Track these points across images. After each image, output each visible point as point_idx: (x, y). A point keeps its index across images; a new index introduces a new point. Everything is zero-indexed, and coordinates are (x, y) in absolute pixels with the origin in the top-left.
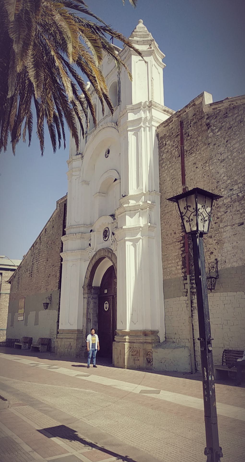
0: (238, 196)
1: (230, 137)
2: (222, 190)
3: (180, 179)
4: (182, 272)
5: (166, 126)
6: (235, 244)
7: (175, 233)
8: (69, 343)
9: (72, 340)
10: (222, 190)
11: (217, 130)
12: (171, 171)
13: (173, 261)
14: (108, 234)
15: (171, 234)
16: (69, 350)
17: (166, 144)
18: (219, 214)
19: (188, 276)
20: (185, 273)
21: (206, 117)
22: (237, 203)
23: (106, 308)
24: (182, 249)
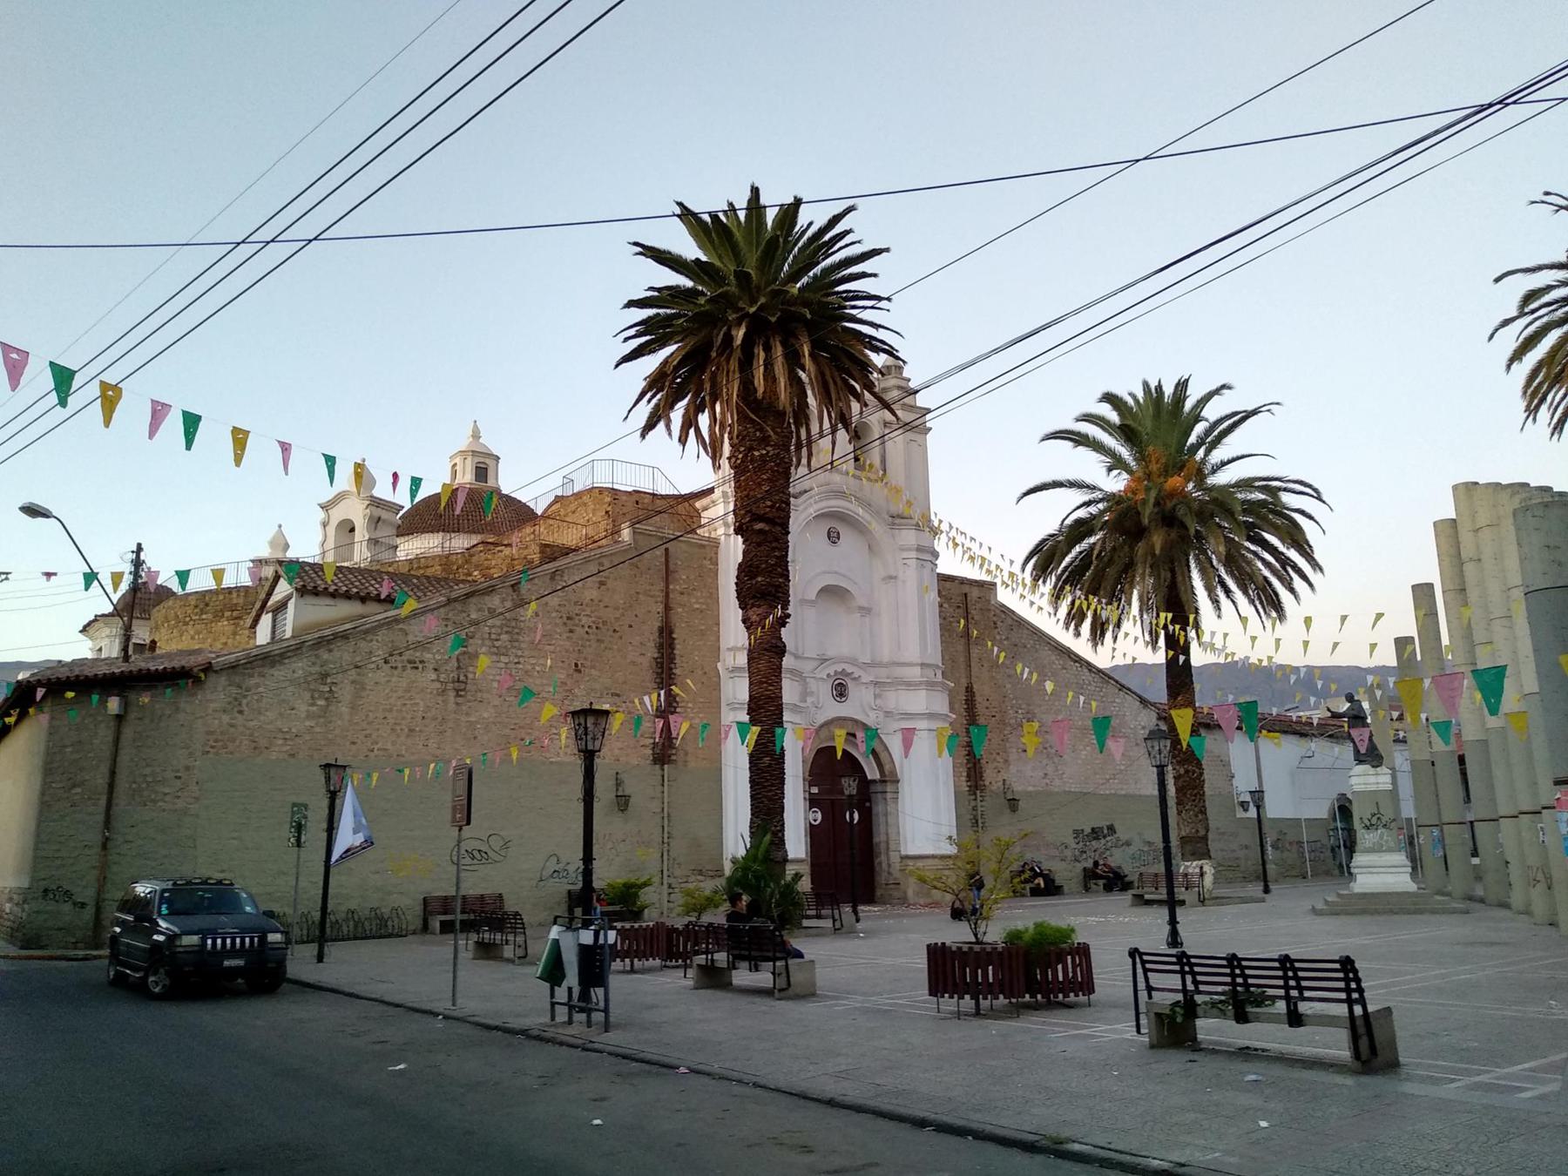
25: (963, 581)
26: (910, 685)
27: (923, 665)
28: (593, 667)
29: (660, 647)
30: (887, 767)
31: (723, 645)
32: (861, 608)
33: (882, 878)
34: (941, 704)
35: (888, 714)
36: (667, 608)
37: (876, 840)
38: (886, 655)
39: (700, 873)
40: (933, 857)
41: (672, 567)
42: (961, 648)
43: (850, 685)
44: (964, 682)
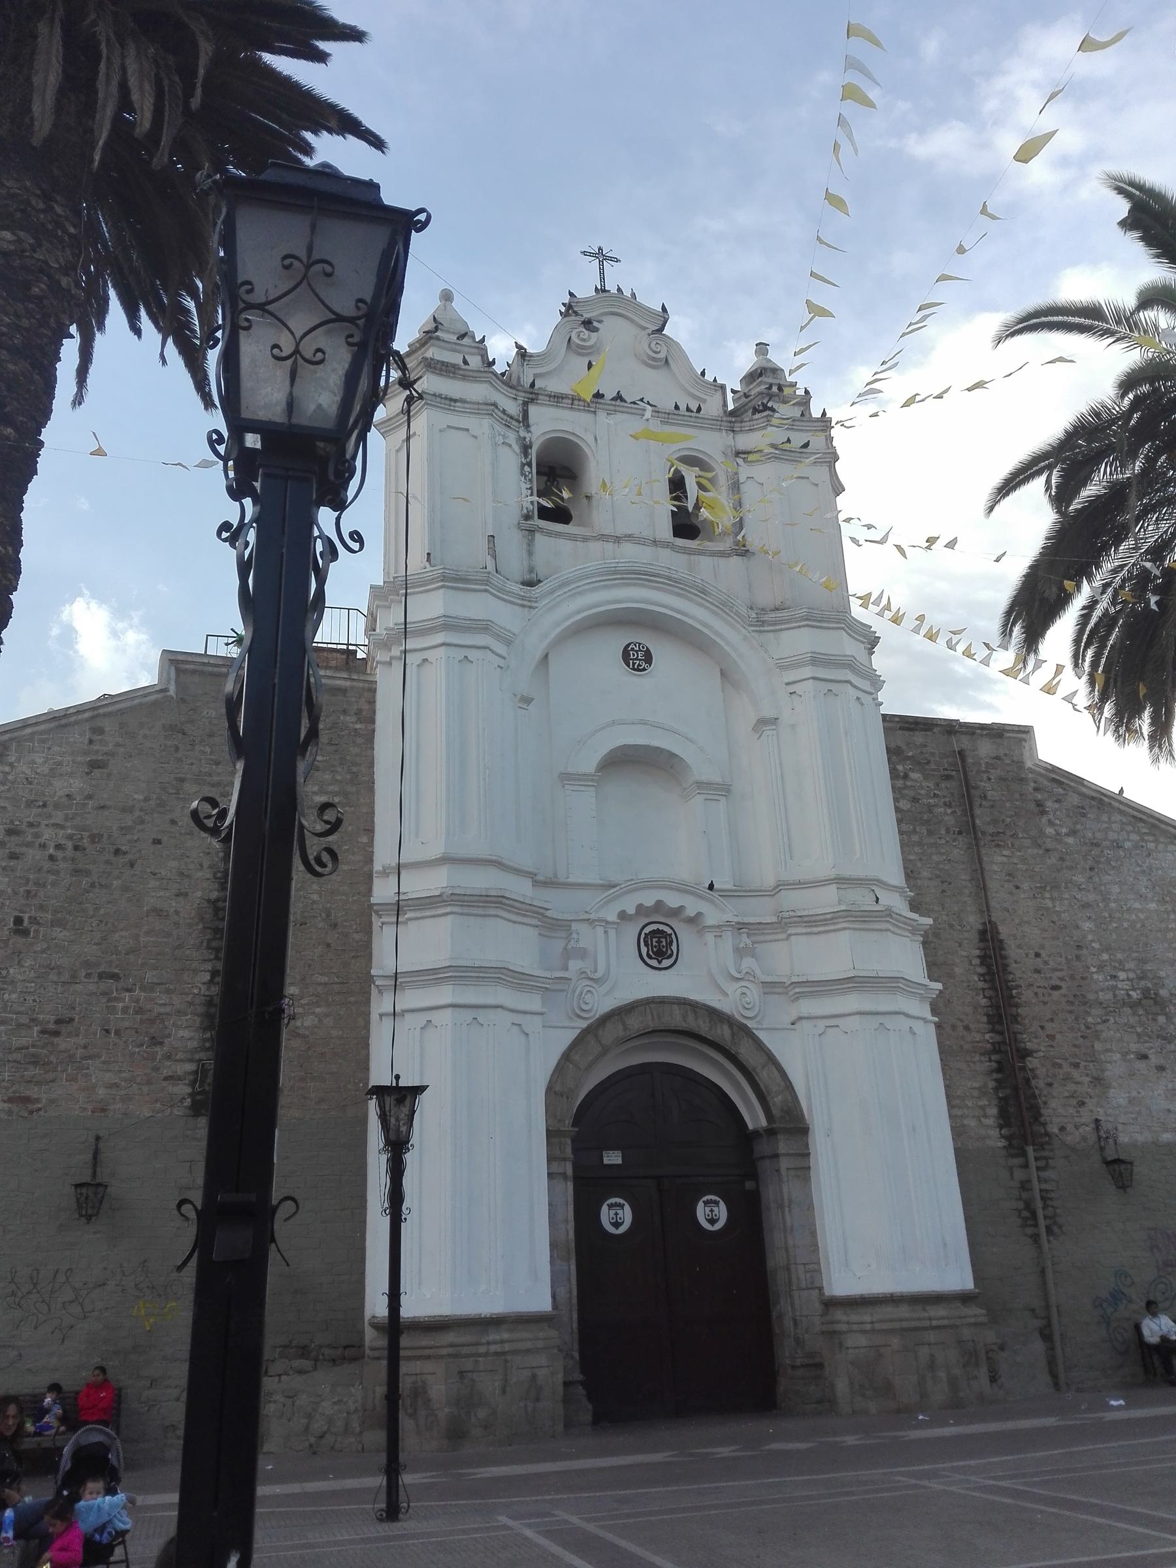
0: (1128, 995)
1: (1098, 862)
3: (967, 891)
4: (1002, 1136)
6: (1134, 1094)
7: (967, 1028)
9: (542, 1360)
10: (1094, 970)
11: (1064, 830)
12: (935, 858)
14: (674, 948)
15: (954, 1027)
17: (906, 777)
19: (1030, 1149)
23: (617, 1225)
24: (995, 1076)
26: (813, 923)
27: (841, 881)
28: (57, 923)
30: (778, 1099)
33: (786, 1353)
34: (905, 958)
35: (770, 987)
37: (770, 1264)
38: (765, 873)
39: (304, 1352)
43: (686, 937)
44: (973, 921)
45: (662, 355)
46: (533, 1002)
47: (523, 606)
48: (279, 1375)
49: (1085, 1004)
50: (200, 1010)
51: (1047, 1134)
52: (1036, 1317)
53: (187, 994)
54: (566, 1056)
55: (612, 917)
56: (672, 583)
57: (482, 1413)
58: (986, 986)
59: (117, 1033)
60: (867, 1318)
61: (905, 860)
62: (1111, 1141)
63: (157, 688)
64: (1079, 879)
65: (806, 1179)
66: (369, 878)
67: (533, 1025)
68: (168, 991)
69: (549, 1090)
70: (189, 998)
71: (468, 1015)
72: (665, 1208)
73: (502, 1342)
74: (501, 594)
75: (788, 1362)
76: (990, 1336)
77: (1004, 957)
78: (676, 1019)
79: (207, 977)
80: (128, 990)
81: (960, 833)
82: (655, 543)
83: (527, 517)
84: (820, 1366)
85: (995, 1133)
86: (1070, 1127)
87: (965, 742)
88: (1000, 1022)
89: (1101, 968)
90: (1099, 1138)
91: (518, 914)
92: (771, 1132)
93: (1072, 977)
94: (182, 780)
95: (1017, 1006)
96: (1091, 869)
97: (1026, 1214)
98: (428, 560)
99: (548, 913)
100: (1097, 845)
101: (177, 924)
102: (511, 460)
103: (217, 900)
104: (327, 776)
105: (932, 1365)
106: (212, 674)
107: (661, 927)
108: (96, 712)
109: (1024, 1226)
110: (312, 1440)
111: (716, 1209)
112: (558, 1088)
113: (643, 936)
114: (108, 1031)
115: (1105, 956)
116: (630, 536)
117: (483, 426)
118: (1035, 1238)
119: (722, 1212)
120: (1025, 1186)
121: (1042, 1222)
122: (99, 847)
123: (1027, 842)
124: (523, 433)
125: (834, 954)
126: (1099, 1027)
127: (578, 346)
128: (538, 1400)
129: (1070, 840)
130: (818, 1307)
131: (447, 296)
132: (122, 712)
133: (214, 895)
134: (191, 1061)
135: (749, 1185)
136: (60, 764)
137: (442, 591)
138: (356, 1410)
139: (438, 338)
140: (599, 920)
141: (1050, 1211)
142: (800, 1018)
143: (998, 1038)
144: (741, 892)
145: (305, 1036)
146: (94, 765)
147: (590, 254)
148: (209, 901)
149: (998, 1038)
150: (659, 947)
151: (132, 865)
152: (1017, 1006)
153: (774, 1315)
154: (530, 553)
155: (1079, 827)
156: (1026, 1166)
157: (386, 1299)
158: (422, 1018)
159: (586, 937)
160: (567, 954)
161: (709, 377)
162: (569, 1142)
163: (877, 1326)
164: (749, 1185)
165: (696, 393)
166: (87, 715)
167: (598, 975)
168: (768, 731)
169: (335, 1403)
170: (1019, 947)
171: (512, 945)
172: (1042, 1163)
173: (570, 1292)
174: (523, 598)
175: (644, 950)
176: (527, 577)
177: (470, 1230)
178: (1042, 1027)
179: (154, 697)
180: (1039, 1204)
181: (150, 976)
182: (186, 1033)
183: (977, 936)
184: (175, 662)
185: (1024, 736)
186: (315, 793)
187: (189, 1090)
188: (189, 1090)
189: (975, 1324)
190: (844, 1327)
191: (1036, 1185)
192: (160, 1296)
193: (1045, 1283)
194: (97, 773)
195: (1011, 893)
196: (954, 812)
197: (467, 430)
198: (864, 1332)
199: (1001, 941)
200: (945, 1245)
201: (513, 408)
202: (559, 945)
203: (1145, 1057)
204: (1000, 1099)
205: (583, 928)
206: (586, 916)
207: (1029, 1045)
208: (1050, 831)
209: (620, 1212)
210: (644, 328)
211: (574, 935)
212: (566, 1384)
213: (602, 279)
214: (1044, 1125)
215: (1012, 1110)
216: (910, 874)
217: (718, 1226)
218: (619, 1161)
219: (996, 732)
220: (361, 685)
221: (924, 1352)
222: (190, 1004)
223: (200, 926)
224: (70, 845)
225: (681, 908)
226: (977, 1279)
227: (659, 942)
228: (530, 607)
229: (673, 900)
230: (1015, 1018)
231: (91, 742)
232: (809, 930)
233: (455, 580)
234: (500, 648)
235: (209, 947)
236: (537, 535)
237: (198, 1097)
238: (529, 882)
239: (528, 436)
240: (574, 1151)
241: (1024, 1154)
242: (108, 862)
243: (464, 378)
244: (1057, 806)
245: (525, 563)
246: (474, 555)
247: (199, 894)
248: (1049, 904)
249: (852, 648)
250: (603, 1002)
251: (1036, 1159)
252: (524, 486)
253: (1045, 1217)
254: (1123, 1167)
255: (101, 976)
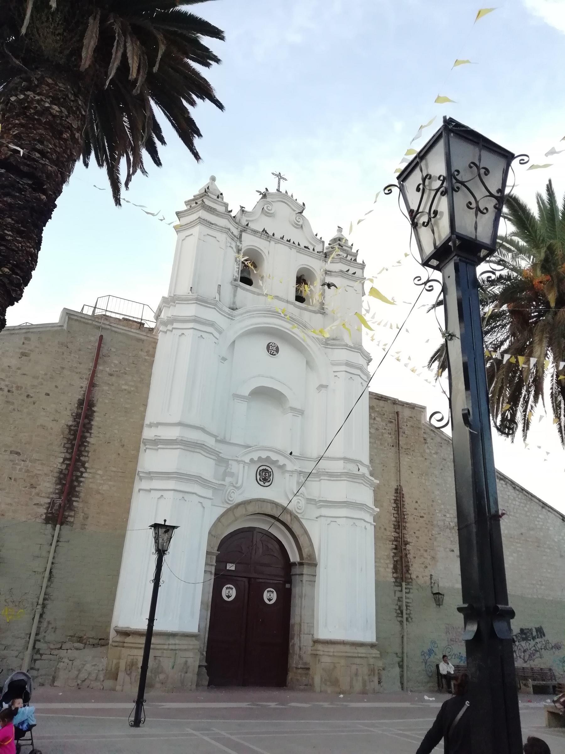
2: (437, 511)
5: (378, 399)
7: (385, 529)
8: (184, 660)
9: (191, 654)
10: (437, 511)
11: (433, 452)
13: (382, 561)
14: (271, 478)
16: (183, 675)
17: (374, 419)
18: (433, 532)
19: (404, 584)
20: (396, 578)
21: (423, 431)
22: (448, 530)
23: (228, 597)
25: (395, 402)
26: (332, 476)
27: (346, 460)
29: (77, 416)
30: (305, 551)
31: (147, 421)
32: (293, 409)
33: (294, 662)
34: (366, 496)
35: (310, 501)
36: (92, 385)
37: (292, 621)
39: (80, 640)
40: (343, 643)
41: (104, 351)
42: (391, 453)
44: (394, 485)
45: (300, 223)
46: (208, 493)
47: (229, 318)
48: (67, 650)
49: (432, 525)
50: (56, 475)
51: (411, 578)
52: (397, 657)
53: (50, 467)
54: (219, 520)
55: (247, 461)
56: (293, 320)
57: (162, 676)
58: (395, 512)
59: (15, 480)
60: (332, 650)
61: (370, 455)
62: (436, 585)
63: (59, 325)
64: (436, 472)
65: (313, 586)
66: (142, 426)
67: (207, 503)
68: (42, 464)
69: (210, 533)
70: (51, 469)
71: (180, 495)
72: (251, 592)
73: (175, 644)
74: (220, 311)
75: (294, 666)
76: (380, 664)
77: (403, 501)
78: (268, 510)
79: (61, 460)
80: (23, 461)
81: (393, 446)
82: (288, 302)
83: (235, 280)
84: (308, 669)
85: (391, 575)
86: (420, 577)
87: (398, 408)
88: (399, 529)
89: (440, 511)
90: (431, 583)
91: (208, 453)
92: (301, 564)
93: (429, 513)
94: (63, 368)
95: (406, 522)
96: (442, 469)
97: (399, 611)
98: (191, 290)
99: (220, 455)
100: (445, 460)
101: (51, 434)
102: (232, 254)
103: (71, 426)
104: (129, 378)
105: (356, 675)
106: (84, 323)
107: (267, 468)
108: (28, 330)
109: (397, 617)
110: (79, 682)
111: (272, 595)
112: (213, 533)
113: (259, 471)
114: (10, 478)
115: (442, 506)
116: (277, 297)
117: (222, 237)
118: (401, 622)
119: (274, 596)
120: (400, 599)
121: (405, 616)
122: (19, 392)
123: (419, 454)
124: (238, 244)
125: (338, 490)
126: (436, 536)
127: (266, 212)
128: (186, 673)
129: (435, 456)
130: (311, 643)
131: (213, 179)
132: (40, 332)
133: (70, 423)
134: (48, 498)
135: (288, 586)
136: (7, 351)
137: (195, 305)
138: (103, 670)
139: (208, 196)
140: (242, 461)
141: (408, 611)
142: (321, 516)
143: (397, 535)
144: (302, 458)
145: (103, 494)
146: (24, 354)
147: (276, 175)
148: (67, 425)
149: (397, 535)
150: (265, 477)
151: (34, 403)
152: (406, 522)
153: (291, 644)
154: (235, 296)
155: (439, 451)
156: (401, 591)
157: (147, 622)
158: (159, 494)
159: (235, 467)
160: (226, 474)
161: (318, 237)
162: (215, 557)
163: (335, 654)
164: (288, 586)
165: (312, 242)
166: (24, 331)
167: (238, 485)
168: (323, 390)
169: (93, 665)
170: (410, 498)
171: (203, 466)
172: (407, 591)
173: (206, 624)
174: (229, 315)
175: (258, 477)
176: (232, 306)
177: (165, 593)
178: (415, 533)
179: (56, 328)
180: (404, 608)
181: (35, 456)
182: (48, 485)
183: (394, 491)
184: (68, 314)
185: (422, 410)
186: (123, 384)
187: (46, 511)
188: (46, 511)
189: (375, 657)
190: (321, 653)
191: (404, 600)
192: (16, 606)
193: (403, 642)
194: (24, 358)
195: (409, 475)
196: (392, 437)
197: (215, 238)
198: (330, 656)
199: (403, 494)
200: (367, 621)
201: (236, 232)
202: (221, 470)
203: (453, 551)
204: (394, 561)
205: (234, 464)
206: (236, 459)
207: (409, 540)
208: (428, 451)
209: (231, 591)
210: (294, 211)
211: (230, 466)
212: (200, 666)
213: (279, 186)
214: (410, 574)
215: (398, 566)
216: (371, 461)
217: (272, 602)
218: (234, 569)
219: (412, 407)
220: (151, 339)
221: (354, 667)
222: (52, 471)
223: (62, 436)
224: (6, 389)
225: (277, 461)
226: (377, 638)
227: (265, 474)
228: (232, 319)
229: (274, 457)
230: (405, 528)
231: (23, 343)
232: (329, 478)
233: (201, 301)
234: (216, 334)
235: (64, 447)
236: (239, 288)
237: (49, 515)
238: (214, 439)
239: (240, 245)
240: (216, 562)
241: (401, 586)
242: (23, 400)
243: (217, 215)
244: (432, 441)
245: (232, 300)
246: (210, 291)
247: (63, 422)
248: (424, 481)
249: (361, 361)
250: (238, 498)
251: (406, 588)
252: (236, 266)
253: (406, 614)
254: (440, 596)
255: (11, 452)
